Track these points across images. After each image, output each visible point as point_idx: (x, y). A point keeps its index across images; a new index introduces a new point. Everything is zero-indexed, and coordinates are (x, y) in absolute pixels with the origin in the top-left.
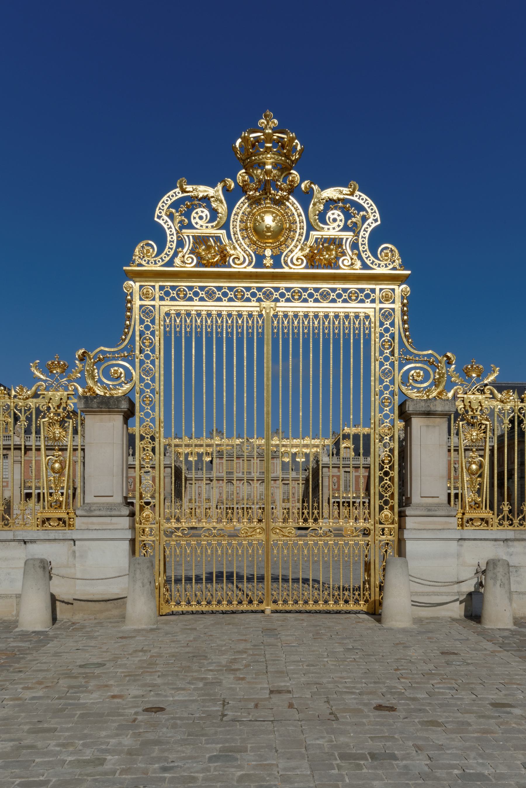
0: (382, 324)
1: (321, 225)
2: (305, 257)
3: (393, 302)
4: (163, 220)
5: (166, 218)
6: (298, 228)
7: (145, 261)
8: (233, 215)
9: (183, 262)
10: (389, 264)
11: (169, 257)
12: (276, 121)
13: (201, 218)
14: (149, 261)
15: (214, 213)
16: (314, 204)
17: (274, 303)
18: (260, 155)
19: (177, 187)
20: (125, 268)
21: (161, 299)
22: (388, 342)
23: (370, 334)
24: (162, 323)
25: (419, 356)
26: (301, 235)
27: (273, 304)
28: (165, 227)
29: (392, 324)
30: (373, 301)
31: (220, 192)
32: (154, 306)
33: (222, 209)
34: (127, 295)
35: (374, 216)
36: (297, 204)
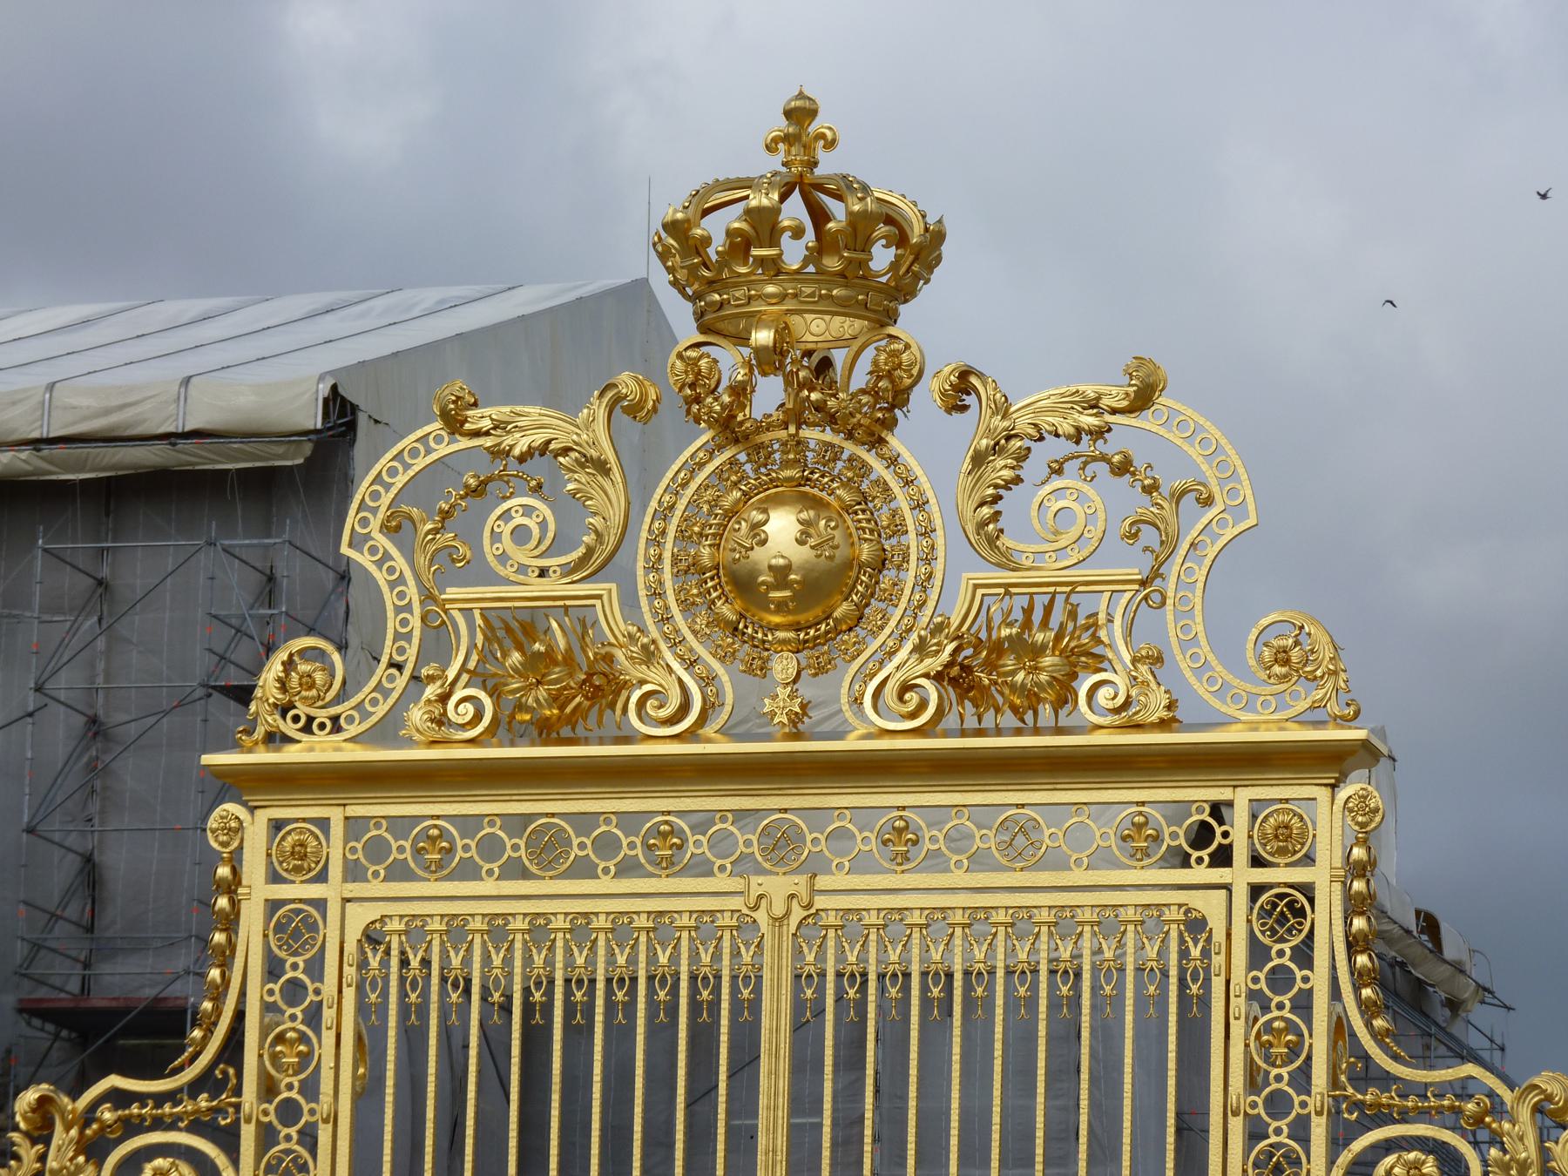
0: (1258, 954)
2: (938, 677)
3: (1309, 860)
4: (373, 550)
5: (382, 541)
9: (441, 721)
11: (391, 701)
13: (521, 535)
14: (310, 719)
17: (802, 879)
18: (737, 285)
21: (353, 872)
22: (1287, 1030)
23: (1205, 1001)
24: (350, 972)
25: (1422, 1091)
29: (1304, 955)
30: (1223, 858)
31: (600, 427)
32: (320, 904)
34: (217, 859)
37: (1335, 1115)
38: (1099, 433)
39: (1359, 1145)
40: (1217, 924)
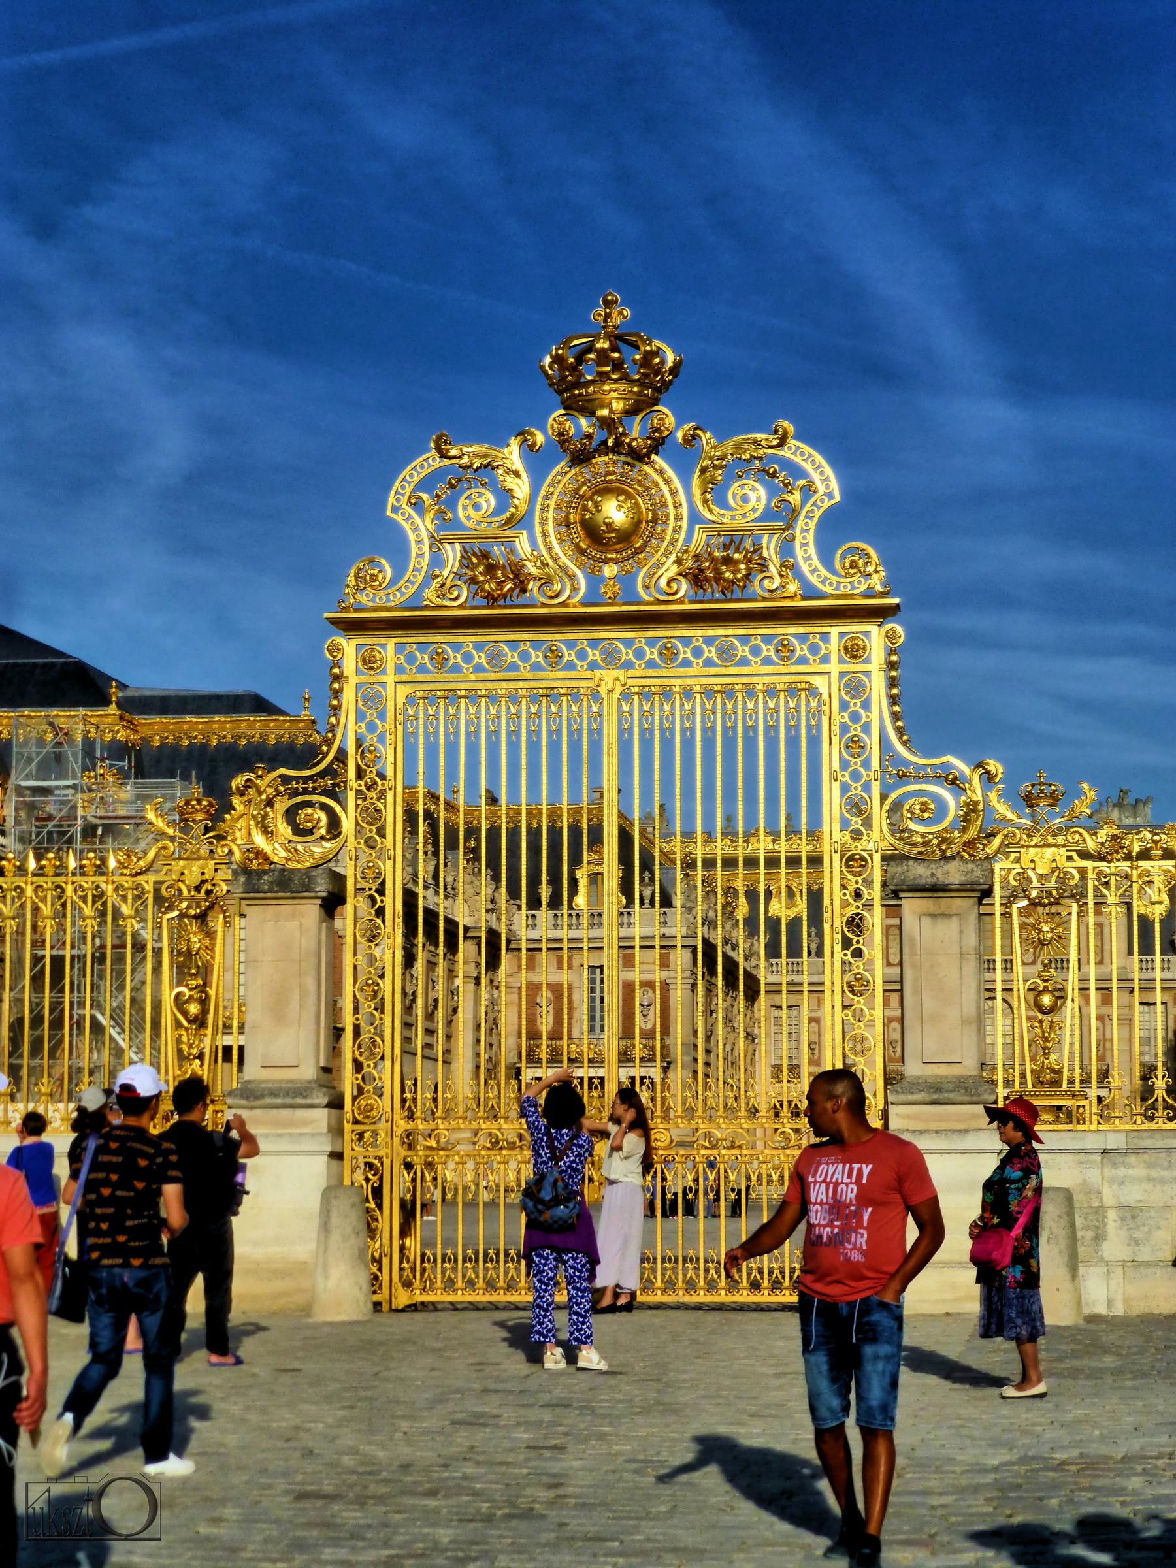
0: (844, 706)
1: (716, 510)
2: (685, 576)
6: (672, 518)
7: (367, 595)
8: (540, 499)
10: (859, 583)
11: (415, 588)
12: (627, 312)
15: (505, 495)
16: (704, 470)
19: (429, 450)
20: (326, 615)
23: (818, 727)
26: (676, 531)
27: (620, 674)
28: (407, 526)
29: (866, 705)
33: (521, 488)
35: (827, 487)
36: (670, 472)
37: (883, 780)
38: (760, 459)
39: (893, 796)
40: (824, 690)
